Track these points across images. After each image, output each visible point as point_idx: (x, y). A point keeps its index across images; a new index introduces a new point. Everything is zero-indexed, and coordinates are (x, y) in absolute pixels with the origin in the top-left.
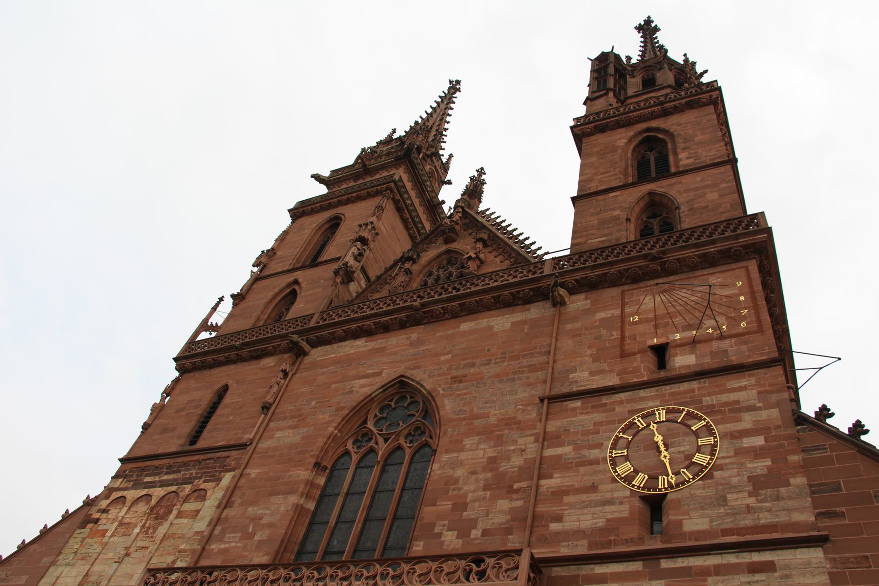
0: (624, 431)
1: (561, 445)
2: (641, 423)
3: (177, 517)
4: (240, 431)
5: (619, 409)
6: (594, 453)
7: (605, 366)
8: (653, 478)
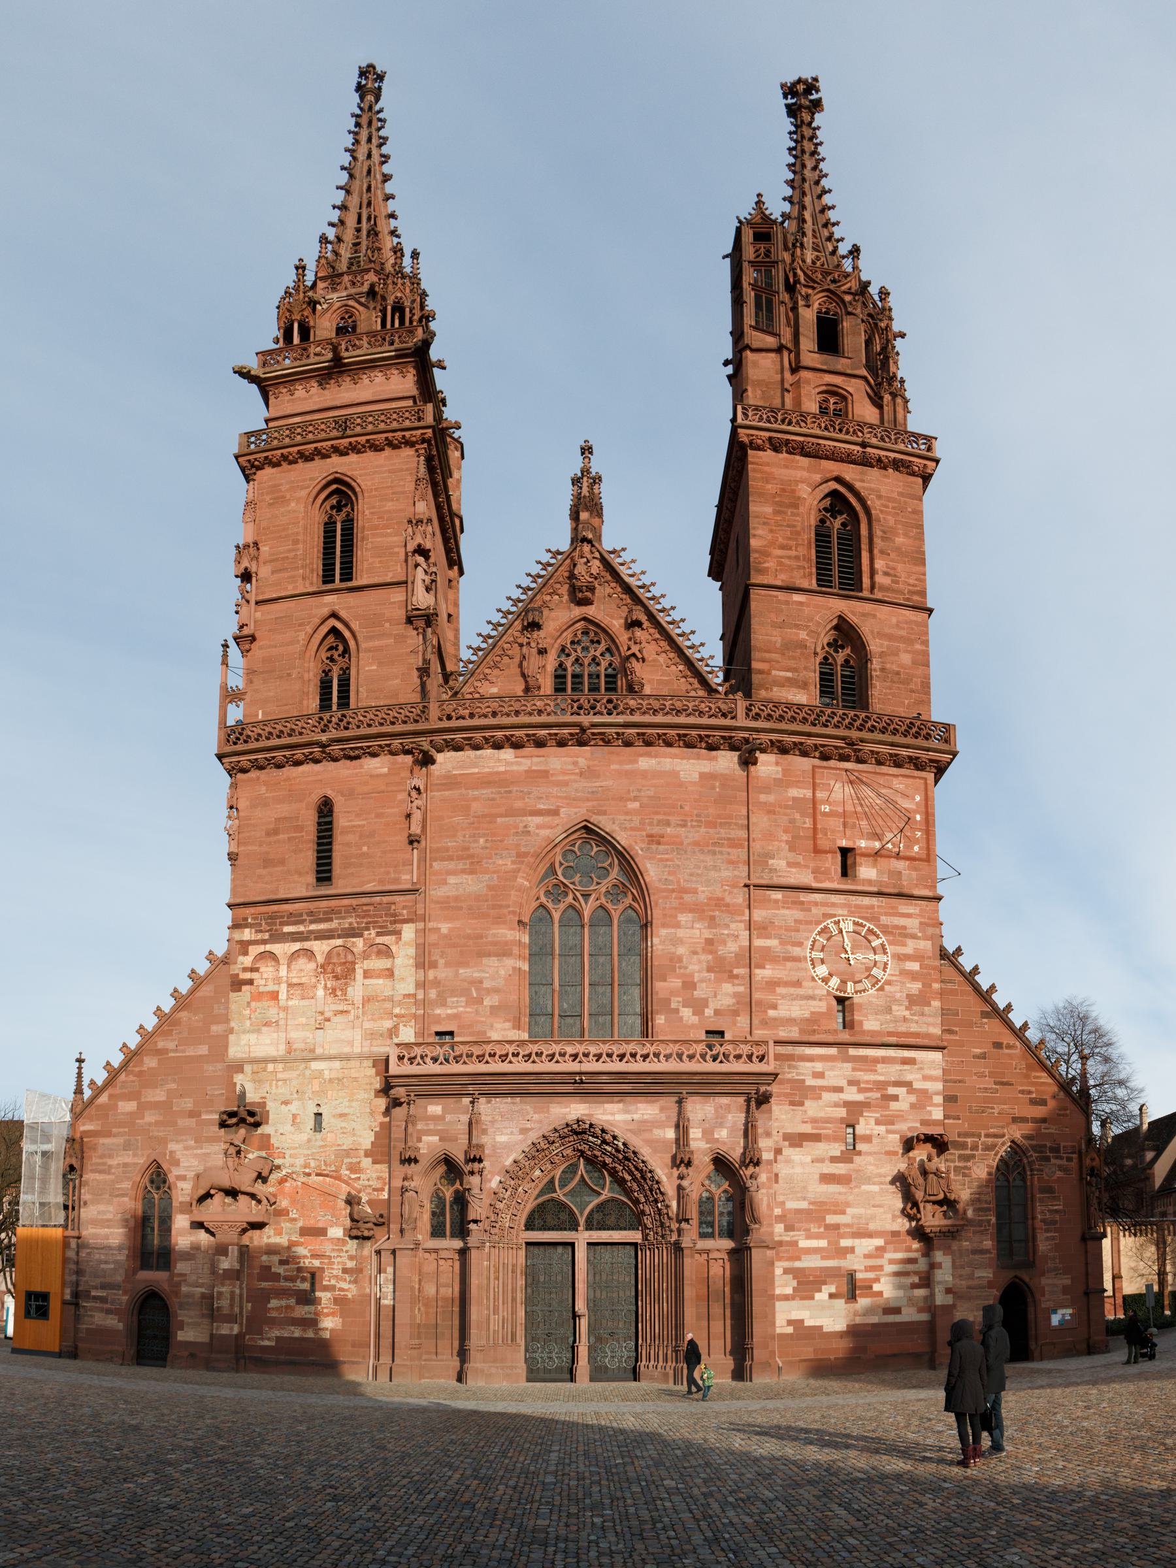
0: (819, 933)
1: (768, 937)
2: (833, 927)
3: (365, 977)
4: (392, 870)
5: (814, 910)
6: (796, 951)
7: (800, 859)
8: (844, 982)
